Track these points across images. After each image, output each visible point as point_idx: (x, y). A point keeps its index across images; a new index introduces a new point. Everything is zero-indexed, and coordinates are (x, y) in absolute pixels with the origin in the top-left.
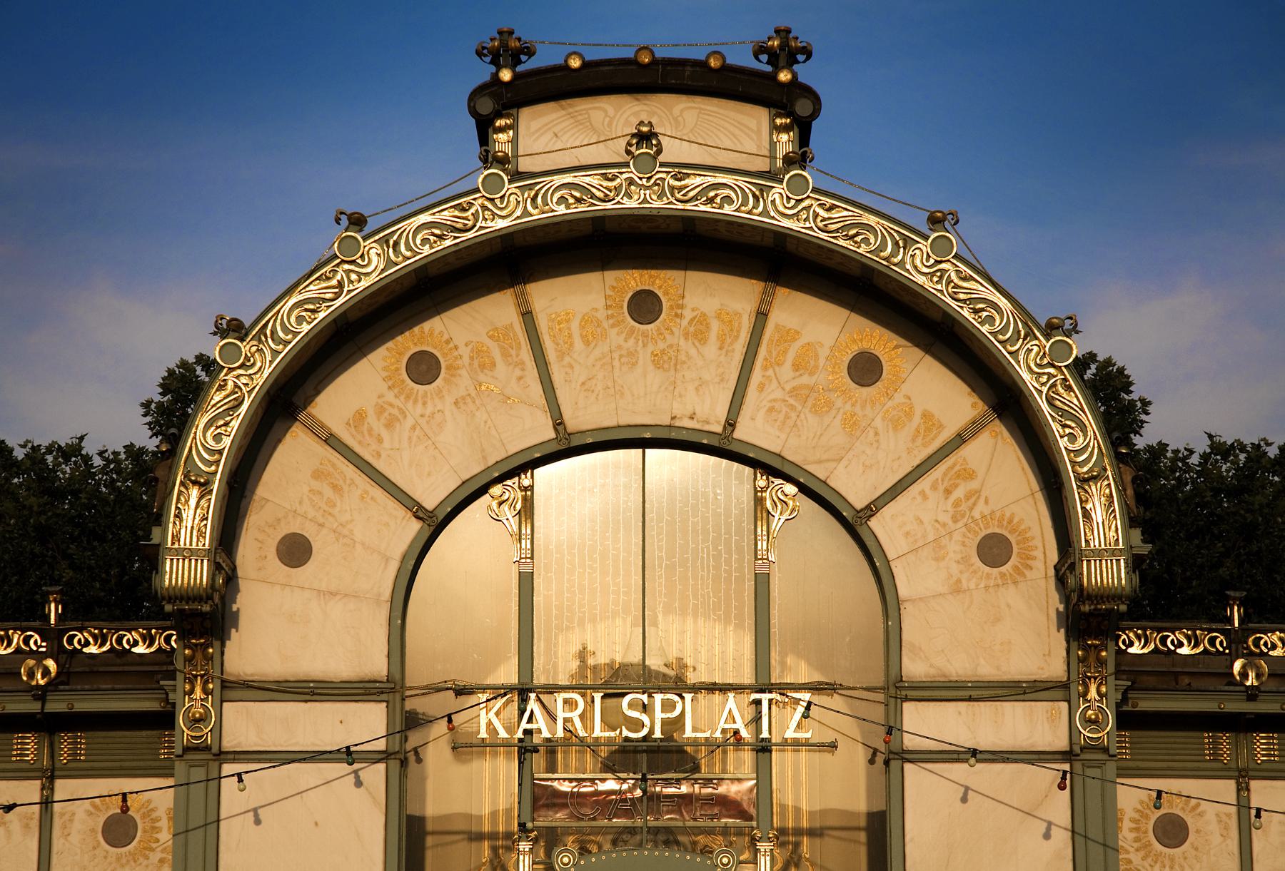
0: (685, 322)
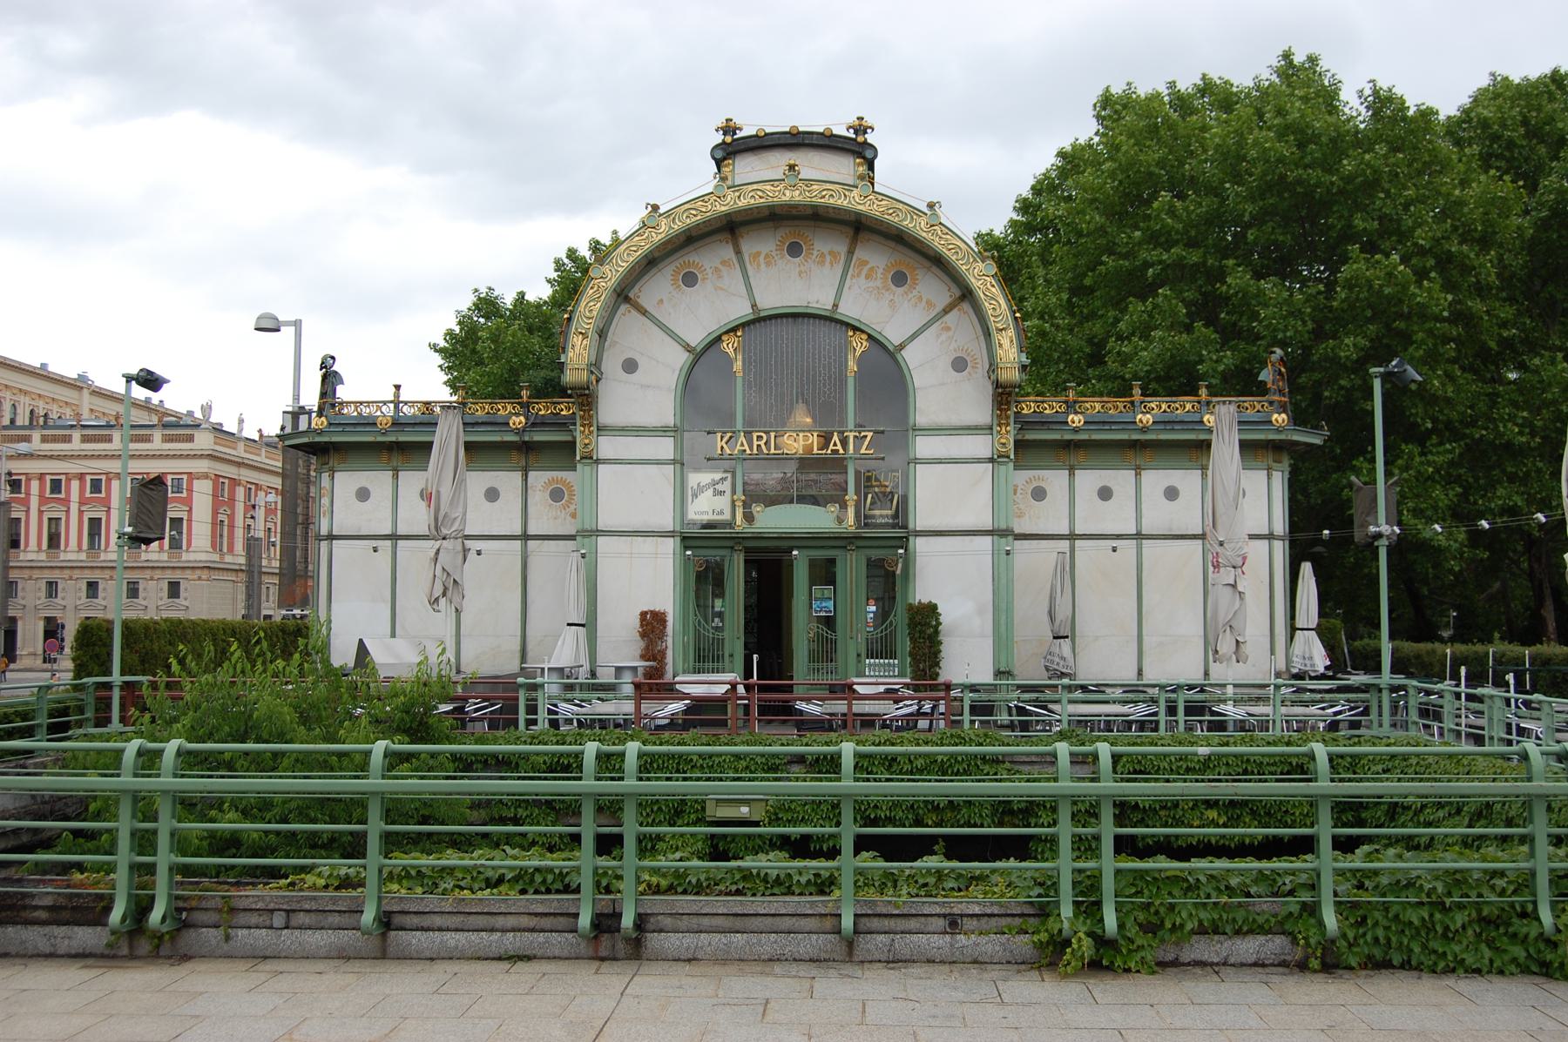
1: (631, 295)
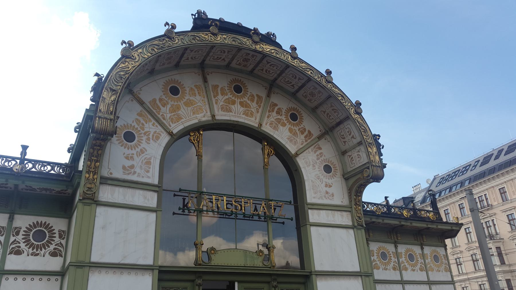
0: (248, 96)
1: (135, 90)
